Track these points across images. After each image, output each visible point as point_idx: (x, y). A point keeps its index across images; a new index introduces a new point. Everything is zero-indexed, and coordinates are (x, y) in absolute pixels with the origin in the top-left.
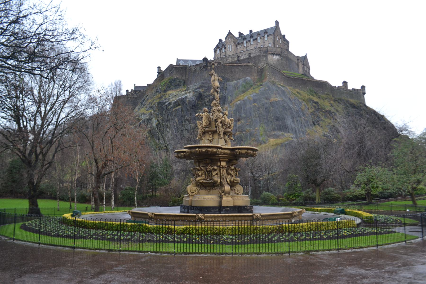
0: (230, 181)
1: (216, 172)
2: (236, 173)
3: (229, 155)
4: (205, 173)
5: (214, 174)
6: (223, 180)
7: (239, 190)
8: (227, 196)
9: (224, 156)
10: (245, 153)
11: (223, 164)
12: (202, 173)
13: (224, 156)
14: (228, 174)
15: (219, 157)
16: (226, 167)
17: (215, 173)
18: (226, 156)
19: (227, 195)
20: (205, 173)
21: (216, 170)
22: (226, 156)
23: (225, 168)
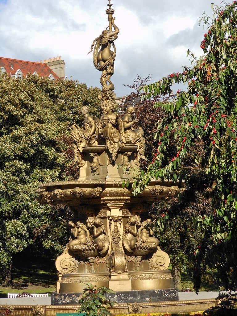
0: (130, 245)
1: (101, 230)
3: (125, 196)
5: (97, 234)
7: (159, 261)
8: (120, 274)
11: (116, 212)
12: (78, 232)
16: (120, 218)
17: (99, 232)
18: (117, 198)
19: (120, 272)
20: (86, 232)
21: (98, 226)
22: (117, 198)
23: (120, 220)
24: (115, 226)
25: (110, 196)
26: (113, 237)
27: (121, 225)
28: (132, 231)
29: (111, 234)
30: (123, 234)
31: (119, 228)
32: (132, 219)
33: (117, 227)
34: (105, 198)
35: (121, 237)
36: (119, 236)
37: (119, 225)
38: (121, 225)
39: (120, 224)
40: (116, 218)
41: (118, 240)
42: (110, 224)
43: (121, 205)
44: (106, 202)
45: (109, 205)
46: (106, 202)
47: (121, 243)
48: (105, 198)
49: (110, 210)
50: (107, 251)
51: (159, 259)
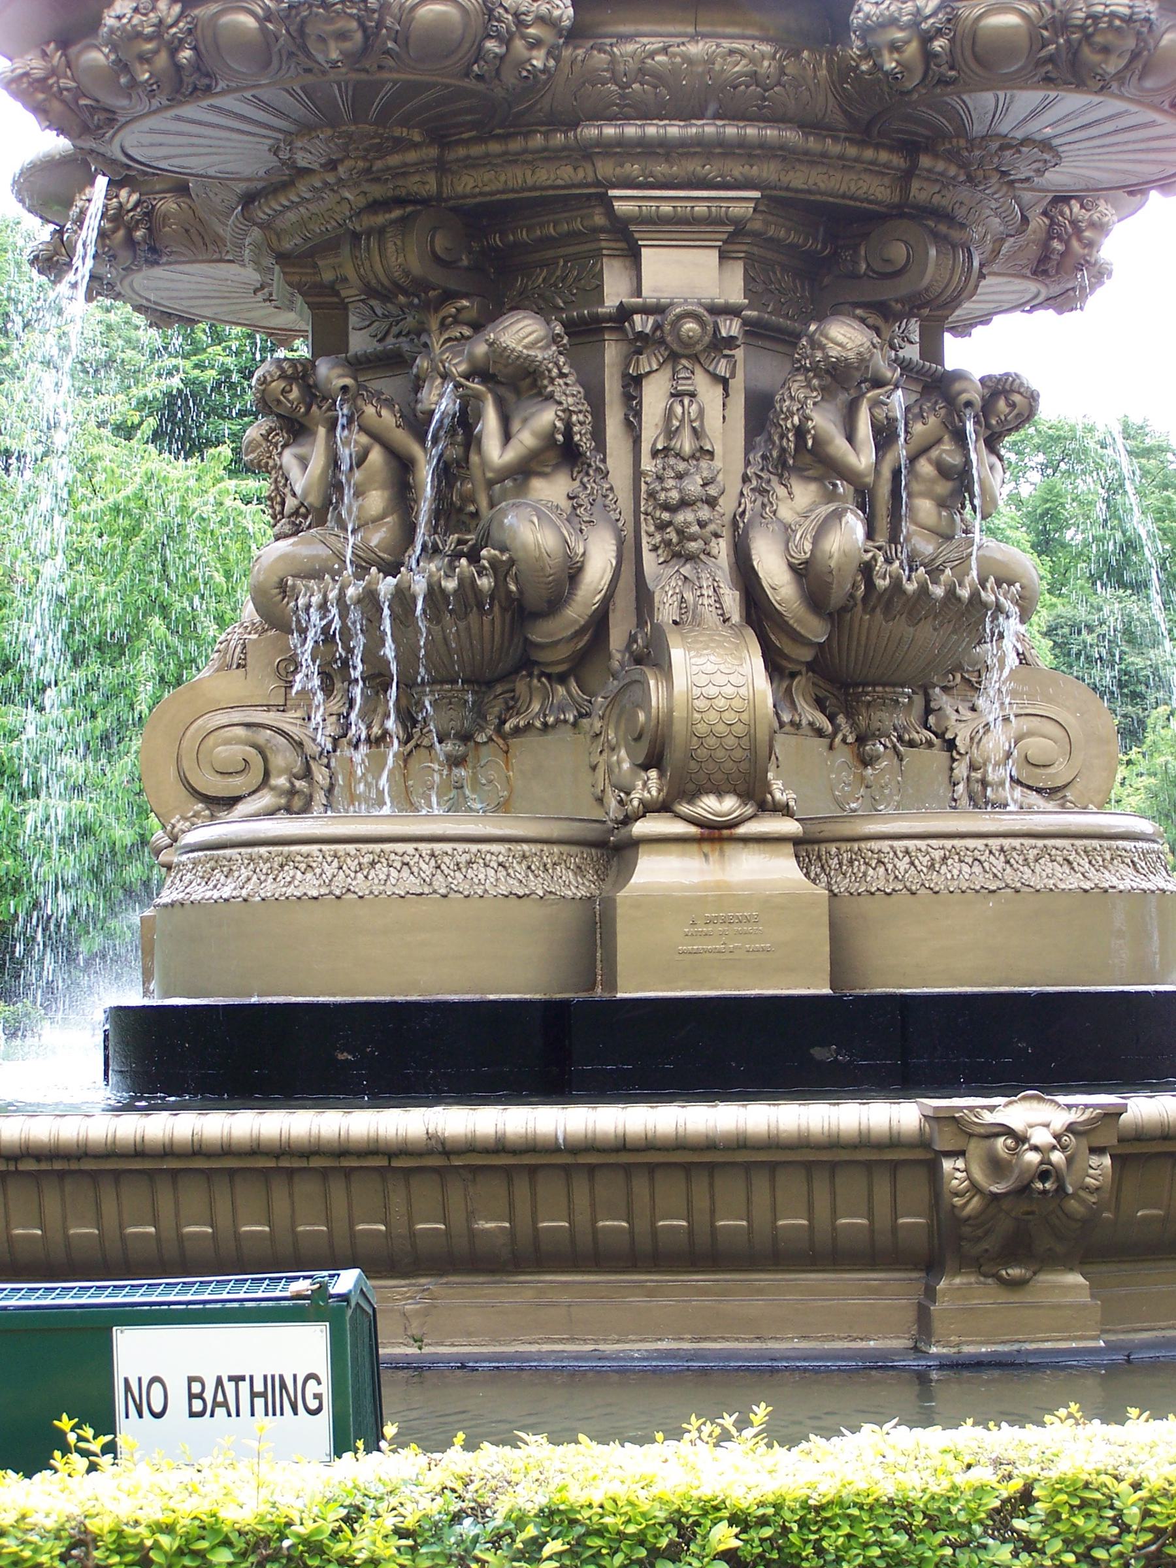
2: (947, 451)
4: (402, 466)
6: (677, 554)
9: (674, 130)
10: (1036, 41)
13: (674, 130)
14: (782, 468)
15: (587, 152)
16: (731, 328)
18: (709, 129)
20: (402, 466)
22: (709, 129)
24: (677, 395)
25: (646, 115)
26: (652, 495)
27: (726, 390)
28: (839, 445)
29: (638, 474)
30: (746, 479)
31: (713, 422)
32: (844, 330)
33: (694, 407)
34: (590, 132)
35: (727, 505)
36: (712, 491)
37: (709, 395)
38: (726, 390)
39: (724, 382)
40: (690, 327)
41: (702, 524)
42: (633, 384)
43: (737, 210)
44: (605, 169)
45: (625, 203)
46: (605, 169)
47: (722, 548)
48: (590, 132)
49: (633, 256)
50: (600, 622)
51: (1030, 734)
